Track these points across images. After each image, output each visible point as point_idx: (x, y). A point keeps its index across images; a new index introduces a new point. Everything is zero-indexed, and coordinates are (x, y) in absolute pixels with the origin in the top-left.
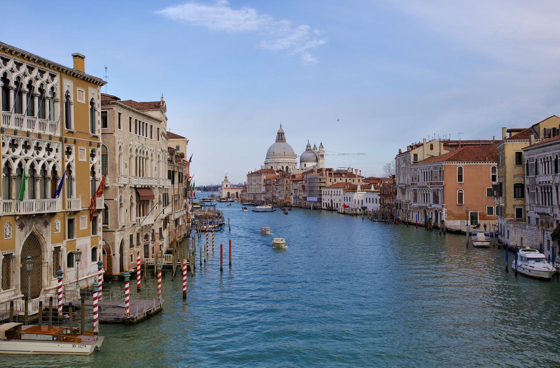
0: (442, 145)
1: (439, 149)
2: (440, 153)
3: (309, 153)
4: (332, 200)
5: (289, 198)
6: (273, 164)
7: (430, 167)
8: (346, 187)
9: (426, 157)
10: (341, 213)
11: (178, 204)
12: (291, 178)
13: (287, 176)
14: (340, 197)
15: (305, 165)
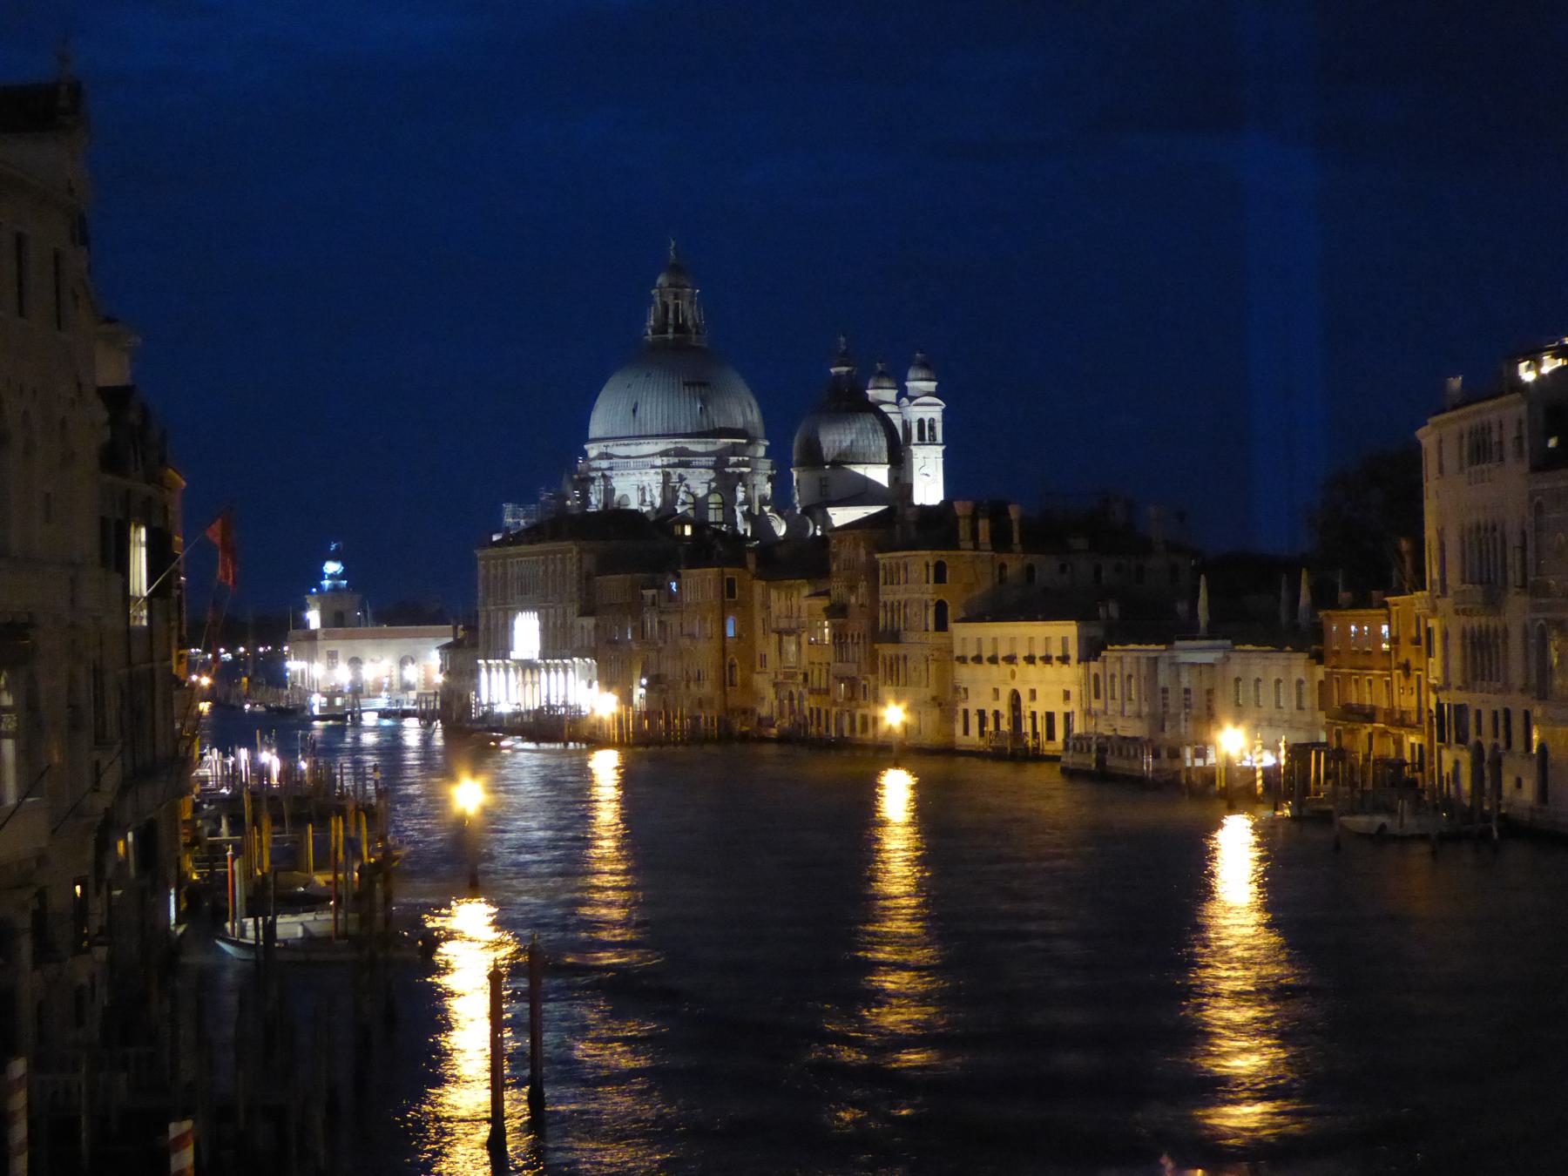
4: (1015, 698)
5: (747, 686)
8: (1101, 611)
14: (1070, 675)
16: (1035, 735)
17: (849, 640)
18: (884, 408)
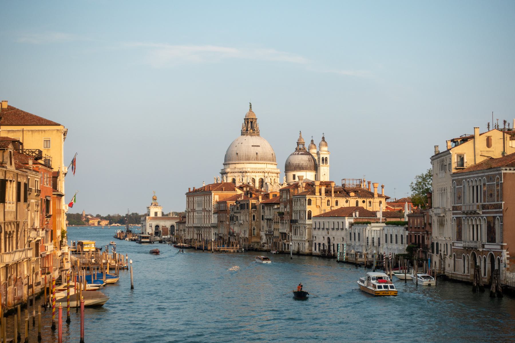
0: (508, 138)
1: (502, 145)
2: (503, 153)
3: (302, 154)
4: (329, 238)
6: (236, 174)
7: (483, 176)
9: (480, 160)
10: (341, 262)
11: (14, 239)
12: (262, 199)
13: (253, 196)
14: (343, 233)
15: (294, 176)
16: (334, 251)
17: (285, 222)
18: (313, 155)
